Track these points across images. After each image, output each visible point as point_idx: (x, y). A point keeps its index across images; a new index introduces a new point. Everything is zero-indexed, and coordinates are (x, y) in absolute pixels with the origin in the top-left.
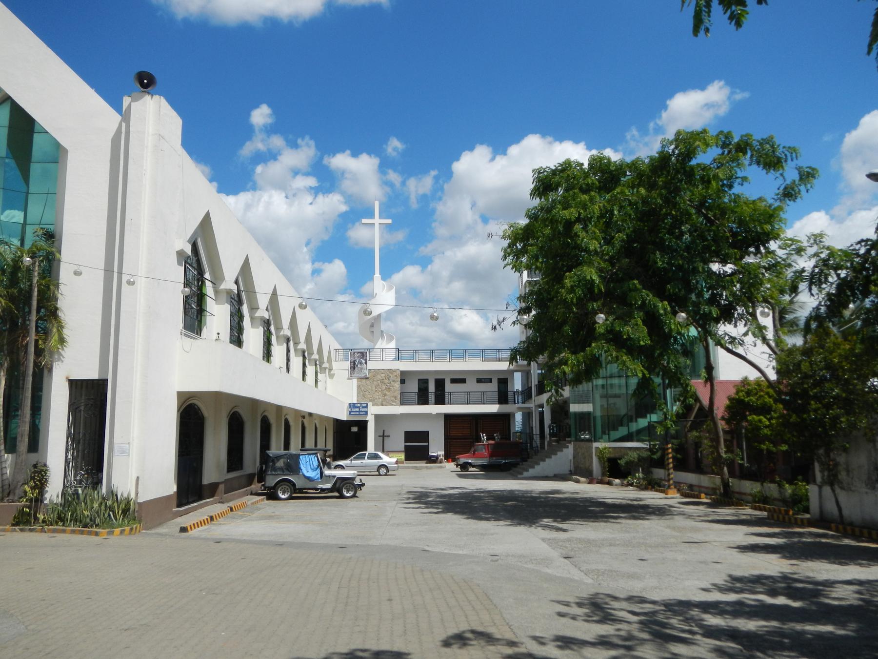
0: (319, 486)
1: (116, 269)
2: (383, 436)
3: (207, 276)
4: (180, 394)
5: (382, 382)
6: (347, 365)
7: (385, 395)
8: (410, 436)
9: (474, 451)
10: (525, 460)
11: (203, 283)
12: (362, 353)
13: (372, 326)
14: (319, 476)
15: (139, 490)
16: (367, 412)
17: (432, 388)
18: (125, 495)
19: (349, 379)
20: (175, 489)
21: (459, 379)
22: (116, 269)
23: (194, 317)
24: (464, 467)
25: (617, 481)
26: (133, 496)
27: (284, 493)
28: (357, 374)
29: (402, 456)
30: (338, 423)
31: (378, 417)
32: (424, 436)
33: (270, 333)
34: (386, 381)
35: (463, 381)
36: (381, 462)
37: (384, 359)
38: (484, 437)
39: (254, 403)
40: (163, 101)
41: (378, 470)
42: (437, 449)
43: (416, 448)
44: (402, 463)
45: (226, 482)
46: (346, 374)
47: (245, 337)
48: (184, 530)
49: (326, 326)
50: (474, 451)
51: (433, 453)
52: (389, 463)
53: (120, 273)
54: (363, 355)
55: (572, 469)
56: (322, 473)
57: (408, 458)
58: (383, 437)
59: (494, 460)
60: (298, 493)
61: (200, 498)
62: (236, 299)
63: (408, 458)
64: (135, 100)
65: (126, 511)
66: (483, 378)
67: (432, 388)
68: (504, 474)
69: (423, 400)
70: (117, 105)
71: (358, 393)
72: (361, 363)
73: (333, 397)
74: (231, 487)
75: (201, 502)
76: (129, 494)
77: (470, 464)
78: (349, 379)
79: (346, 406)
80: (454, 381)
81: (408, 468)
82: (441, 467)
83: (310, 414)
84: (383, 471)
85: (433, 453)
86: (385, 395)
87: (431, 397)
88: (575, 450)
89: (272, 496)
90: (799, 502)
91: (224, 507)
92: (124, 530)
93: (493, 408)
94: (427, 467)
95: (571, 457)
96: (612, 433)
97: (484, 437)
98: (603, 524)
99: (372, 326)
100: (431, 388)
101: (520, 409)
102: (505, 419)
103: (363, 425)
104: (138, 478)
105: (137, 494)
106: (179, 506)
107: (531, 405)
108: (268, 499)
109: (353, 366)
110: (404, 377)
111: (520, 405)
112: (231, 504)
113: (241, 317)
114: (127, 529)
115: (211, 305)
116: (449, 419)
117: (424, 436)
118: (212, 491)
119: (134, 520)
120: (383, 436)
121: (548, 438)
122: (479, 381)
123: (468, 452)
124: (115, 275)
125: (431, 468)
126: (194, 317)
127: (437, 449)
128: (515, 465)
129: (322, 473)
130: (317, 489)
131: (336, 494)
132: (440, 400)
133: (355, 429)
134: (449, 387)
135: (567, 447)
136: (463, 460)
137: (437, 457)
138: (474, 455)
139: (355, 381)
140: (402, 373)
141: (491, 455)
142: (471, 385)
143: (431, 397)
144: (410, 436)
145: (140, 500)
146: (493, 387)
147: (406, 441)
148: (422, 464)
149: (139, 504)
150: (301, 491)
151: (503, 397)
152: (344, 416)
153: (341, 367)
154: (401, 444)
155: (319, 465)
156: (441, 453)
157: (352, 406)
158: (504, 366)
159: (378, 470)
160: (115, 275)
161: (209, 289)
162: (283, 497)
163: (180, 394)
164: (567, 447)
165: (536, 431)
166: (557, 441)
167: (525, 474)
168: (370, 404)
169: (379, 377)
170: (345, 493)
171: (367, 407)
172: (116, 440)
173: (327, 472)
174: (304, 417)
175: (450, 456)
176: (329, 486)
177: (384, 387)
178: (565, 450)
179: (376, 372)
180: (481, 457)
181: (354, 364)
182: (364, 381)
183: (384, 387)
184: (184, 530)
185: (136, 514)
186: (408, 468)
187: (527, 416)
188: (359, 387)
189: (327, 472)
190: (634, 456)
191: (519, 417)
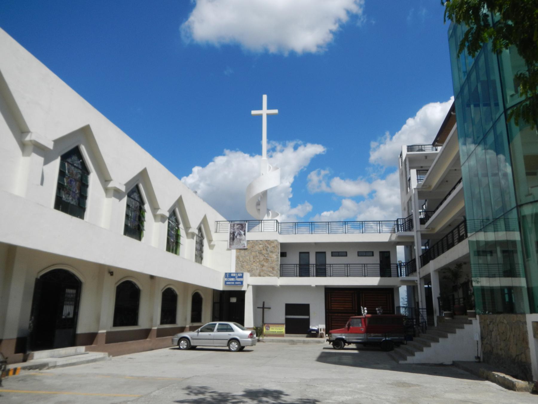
2: (263, 308)
5: (260, 253)
6: (227, 236)
7: (263, 266)
8: (290, 309)
9: (349, 325)
10: (410, 338)
12: (242, 225)
13: (258, 204)
16: (242, 282)
17: (313, 260)
19: (228, 250)
21: (340, 250)
24: (338, 343)
28: (235, 246)
29: (283, 329)
30: (215, 292)
31: (258, 290)
32: (305, 309)
34: (264, 252)
35: (345, 254)
36: (232, 335)
37: (268, 231)
38: (365, 311)
41: (228, 345)
42: (318, 323)
43: (297, 321)
44: (282, 335)
46: (226, 244)
50: (349, 325)
51: (313, 327)
52: (242, 337)
54: (242, 227)
55: (480, 355)
57: (289, 331)
58: (262, 309)
59: (373, 337)
63: (289, 331)
66: (365, 250)
67: (313, 260)
68: (383, 355)
69: (304, 271)
71: (237, 264)
72: (240, 234)
73: (212, 269)
77: (345, 341)
78: (228, 250)
79: (223, 275)
80: (334, 254)
81: (285, 341)
82: (319, 342)
84: (234, 346)
85: (313, 327)
86: (263, 266)
87: (313, 270)
88: (484, 326)
93: (374, 281)
94: (304, 342)
95: (477, 337)
97: (365, 311)
99: (258, 204)
100: (307, 260)
101: (404, 282)
102: (389, 293)
103: (241, 295)
107: (416, 277)
109: (233, 237)
110: (285, 250)
111: (404, 277)
116: (330, 291)
117: (305, 309)
120: (263, 308)
121: (437, 314)
122: (360, 254)
123: (342, 327)
125: (308, 343)
127: (318, 323)
132: (321, 272)
133: (234, 300)
134: (330, 259)
135: (470, 323)
136: (337, 335)
137: (317, 331)
138: (348, 330)
139: (234, 252)
140: (283, 245)
141: (368, 330)
142: (352, 258)
143: (313, 270)
144: (290, 309)
146: (376, 259)
147: (287, 314)
148: (302, 338)
151: (386, 266)
152: (220, 286)
153: (220, 237)
154: (282, 317)
156: (323, 326)
157: (228, 275)
158: (385, 237)
159: (228, 345)
164: (470, 323)
165: (422, 304)
166: (452, 316)
168: (247, 275)
169: (257, 248)
171: (242, 277)
175: (328, 330)
177: (262, 258)
179: (255, 243)
180: (356, 332)
182: (243, 251)
183: (262, 258)
186: (285, 341)
187: (412, 290)
188: (238, 258)
191: (403, 291)
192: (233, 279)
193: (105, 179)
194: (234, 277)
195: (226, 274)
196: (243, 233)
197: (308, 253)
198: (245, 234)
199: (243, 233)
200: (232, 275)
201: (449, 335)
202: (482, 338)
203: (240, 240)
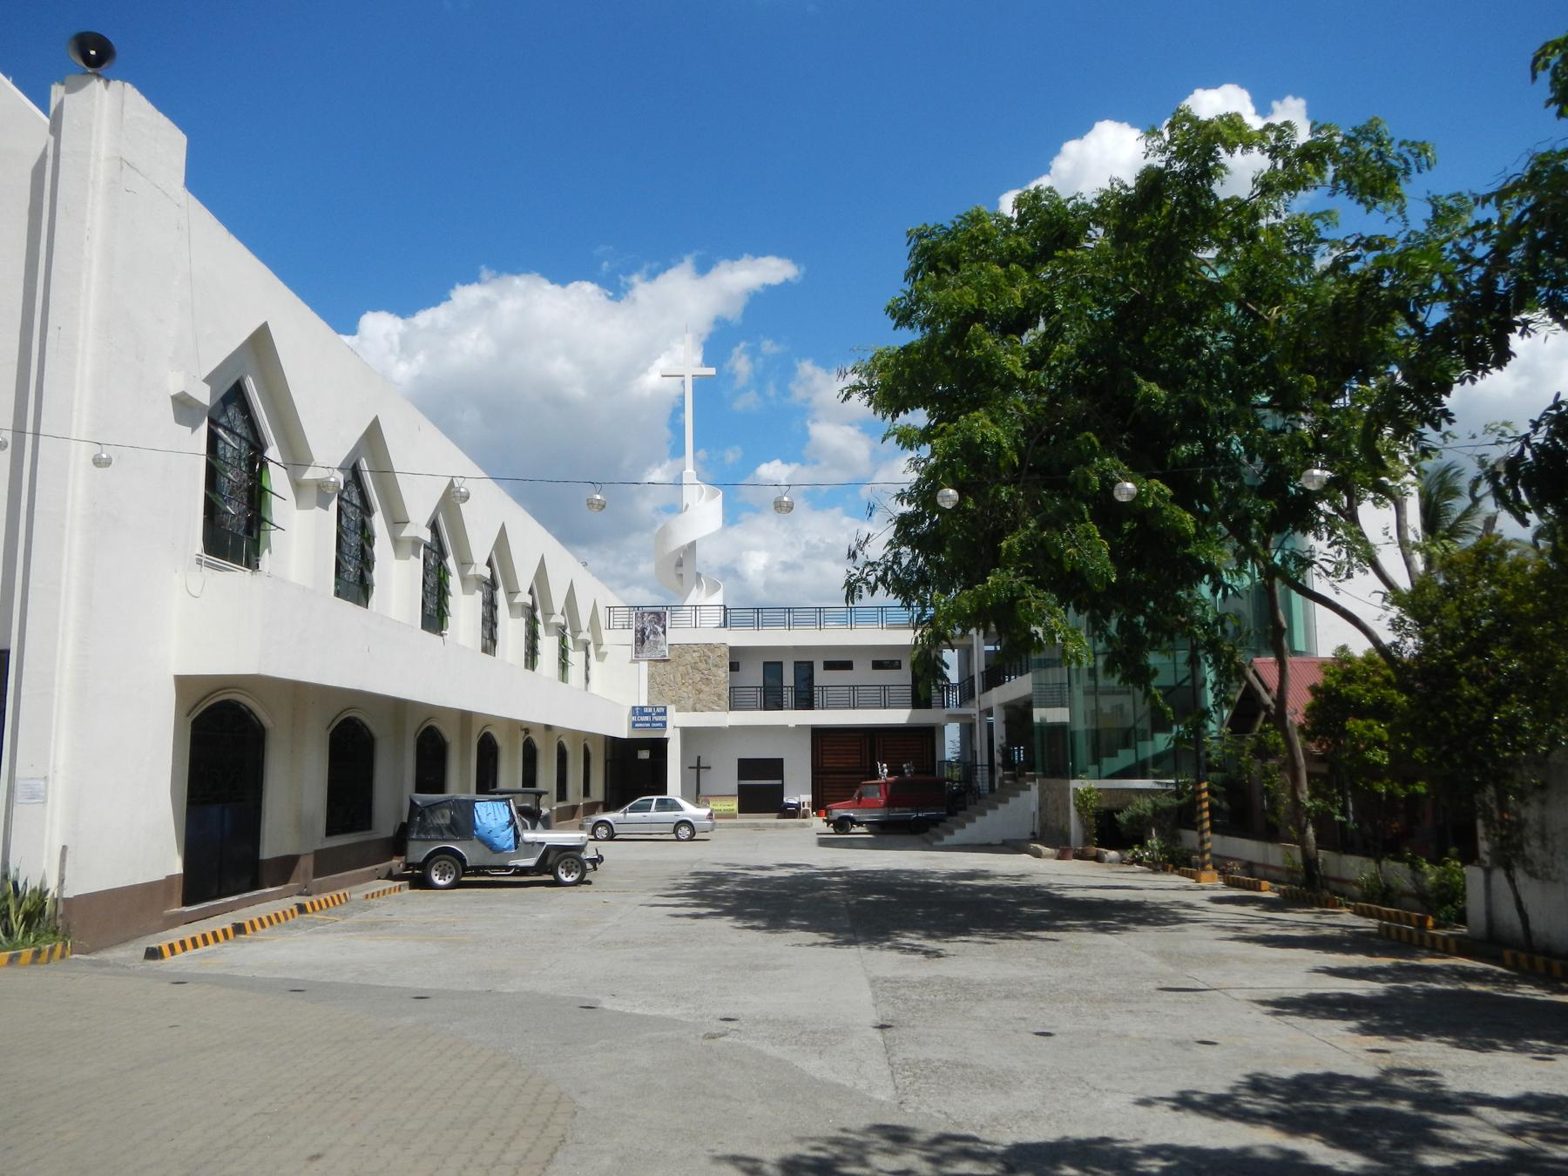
0: (512, 863)
1: (30, 428)
2: (698, 768)
3: (273, 452)
4: (182, 682)
5: (694, 667)
6: (630, 636)
7: (700, 691)
8: (747, 768)
9: (860, 796)
10: (952, 813)
11: (264, 465)
12: (657, 614)
13: (680, 564)
14: (511, 842)
15: (67, 873)
16: (664, 723)
17: (789, 678)
18: (34, 883)
19: (633, 661)
20: (176, 867)
21: (840, 662)
22: (30, 428)
23: (234, 531)
24: (841, 825)
25: (1113, 854)
26: (52, 885)
27: (442, 876)
28: (646, 655)
29: (734, 805)
30: (613, 743)
31: (687, 734)
32: (774, 767)
33: (446, 572)
34: (702, 666)
35: (847, 665)
36: (681, 815)
37: (701, 625)
38: (883, 769)
39: (399, 708)
40: (131, 94)
41: (675, 831)
42: (798, 793)
43: (760, 790)
44: (734, 817)
45: (318, 855)
46: (629, 652)
47: (377, 575)
48: (153, 954)
49: (585, 564)
50: (860, 796)
51: (790, 799)
52: (697, 818)
53: (36, 434)
54: (659, 617)
55: (1037, 830)
56: (517, 836)
57: (743, 809)
58: (696, 769)
59: (897, 813)
60: (469, 876)
61: (255, 885)
62: (356, 501)
63: (743, 809)
64: (71, 90)
65: (33, 917)
66: (884, 661)
67: (789, 678)
68: (915, 838)
69: (772, 700)
70: (42, 101)
71: (650, 688)
72: (655, 633)
73: (603, 697)
74: (329, 864)
75: (247, 895)
76: (43, 883)
77: (853, 821)
78: (633, 661)
79: (628, 711)
80: (829, 666)
81: (743, 826)
82: (803, 825)
83: (548, 728)
84: (684, 832)
85: (790, 799)
86: (700, 691)
87: (788, 696)
88: (1041, 794)
89: (421, 882)
90: (1448, 900)
91: (290, 903)
92: (18, 956)
93: (899, 716)
94: (777, 826)
95: (1034, 807)
96: (1105, 760)
97: (883, 769)
98: (1025, 944)
99: (680, 564)
100: (785, 680)
101: (953, 718)
102: (926, 736)
103: (659, 747)
104: (64, 847)
105: (62, 881)
106: (185, 904)
107: (973, 710)
108: (412, 887)
109: (641, 639)
110: (737, 659)
111: (954, 710)
112: (306, 901)
113: (367, 538)
114: (27, 953)
115: (283, 508)
116: (820, 735)
117: (774, 767)
118: (284, 870)
119: (55, 933)
120: (698, 768)
121: (1000, 772)
122: (878, 665)
123: (849, 797)
124: (29, 439)
125: (784, 827)
126: (234, 531)
127: (798, 793)
128: (941, 820)
129: (517, 836)
130: (508, 868)
131: (551, 878)
132: (805, 700)
133: (644, 755)
134: (821, 677)
135: (1028, 788)
136: (839, 812)
137: (798, 807)
139: (644, 665)
140: (733, 650)
141: (891, 802)
142: (862, 673)
143: (788, 696)
144: (747, 768)
145: (68, 894)
146: (904, 676)
147: (740, 778)
148: (770, 819)
149: (66, 901)
150: (479, 870)
152: (623, 731)
153: (618, 640)
154: (732, 782)
155: (512, 822)
156: (807, 798)
157: (638, 711)
159: (675, 831)
160: (29, 439)
161: (277, 478)
162: (441, 882)
163: (182, 682)
164: (1028, 788)
165: (982, 758)
166: (1014, 778)
167: (948, 839)
168: (671, 709)
169: (688, 658)
170: (563, 877)
171: (664, 714)
172: (19, 773)
173: (528, 836)
174: (527, 731)
175: (819, 805)
176: (531, 862)
177: (698, 677)
178: (1023, 794)
179: (685, 648)
181: (643, 631)
182: (661, 665)
183: (698, 677)
184: (153, 954)
185: (59, 922)
186: (743, 826)
188: (651, 677)
189: (528, 836)
190: (1145, 805)
192: (647, 718)
193: (512, 593)
196: (660, 630)
201: (1001, 806)
202: (1040, 809)
203: (656, 643)
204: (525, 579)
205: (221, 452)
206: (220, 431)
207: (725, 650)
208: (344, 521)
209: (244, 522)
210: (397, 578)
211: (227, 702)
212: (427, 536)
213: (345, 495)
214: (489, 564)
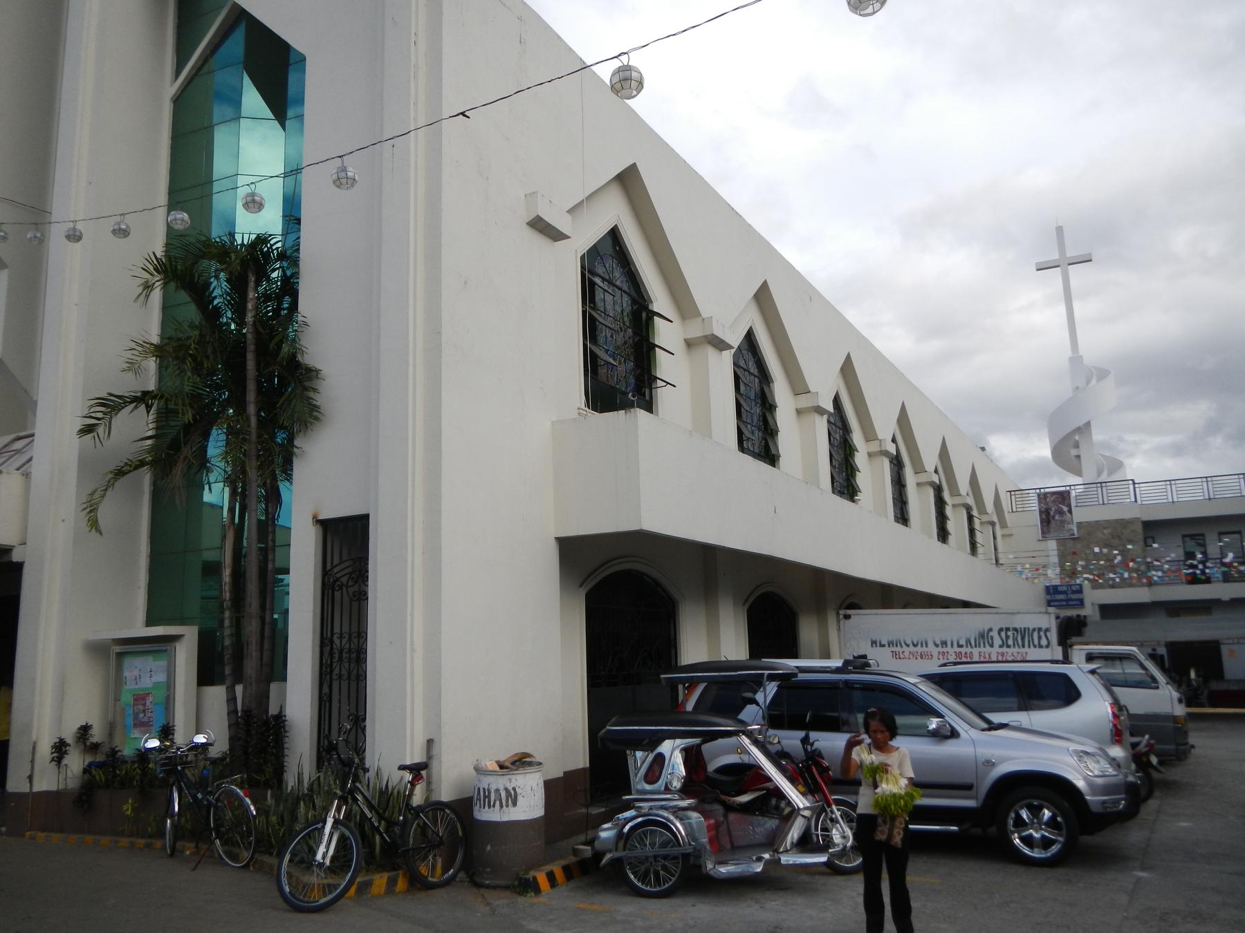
62: (754, 370)
72: (1061, 512)
104: (430, 743)
113: (767, 405)
115: (670, 365)
171: (1080, 591)
192: (1062, 597)
194: (1061, 593)
195: (1047, 587)
196: (1065, 509)
197: (1203, 535)
198: (1070, 511)
199: (1065, 509)
200: (1060, 589)
203: (1063, 522)
204: (930, 459)
205: (600, 304)
206: (597, 280)
207: (1139, 528)
208: (742, 388)
209: (632, 381)
210: (802, 440)
211: (628, 573)
212: (830, 408)
213: (742, 363)
214: (894, 440)
